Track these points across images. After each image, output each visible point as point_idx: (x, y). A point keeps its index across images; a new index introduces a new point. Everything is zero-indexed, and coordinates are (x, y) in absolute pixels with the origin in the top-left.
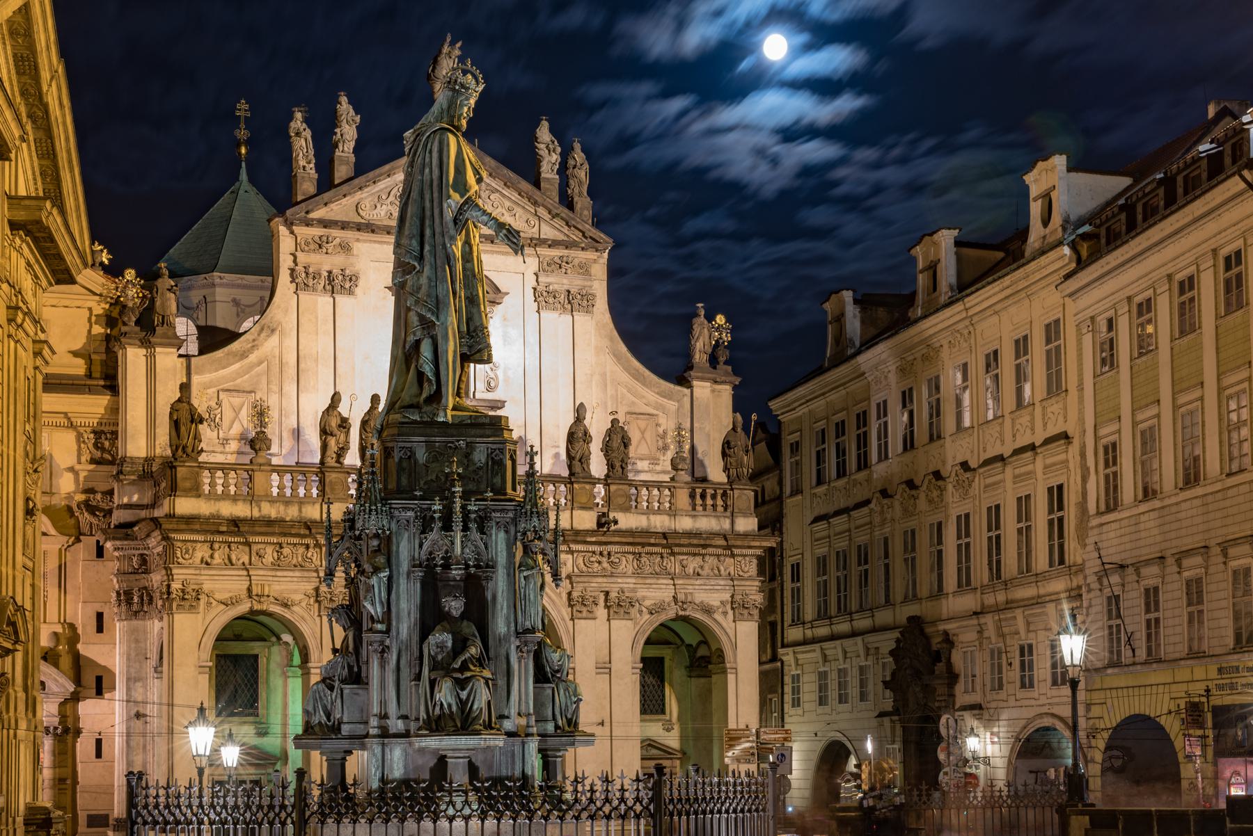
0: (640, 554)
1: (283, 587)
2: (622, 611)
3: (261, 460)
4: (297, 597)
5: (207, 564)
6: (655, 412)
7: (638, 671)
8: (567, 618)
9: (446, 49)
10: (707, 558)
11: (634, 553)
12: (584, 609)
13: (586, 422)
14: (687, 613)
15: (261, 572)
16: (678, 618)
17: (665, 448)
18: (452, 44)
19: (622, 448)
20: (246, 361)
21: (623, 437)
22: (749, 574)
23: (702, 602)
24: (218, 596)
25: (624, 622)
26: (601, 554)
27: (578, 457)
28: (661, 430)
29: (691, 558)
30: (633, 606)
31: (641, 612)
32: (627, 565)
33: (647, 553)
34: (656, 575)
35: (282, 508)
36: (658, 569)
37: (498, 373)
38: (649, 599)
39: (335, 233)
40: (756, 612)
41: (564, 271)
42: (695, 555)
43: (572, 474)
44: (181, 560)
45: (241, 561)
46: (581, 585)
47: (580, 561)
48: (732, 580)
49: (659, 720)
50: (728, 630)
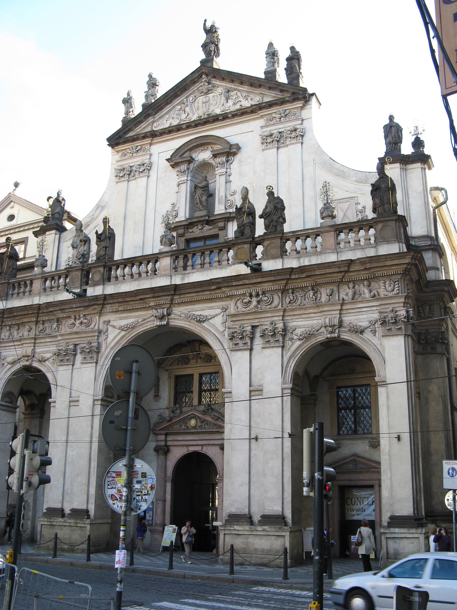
1: (41, 350)
4: (47, 355)
7: (289, 391)
10: (351, 285)
15: (28, 341)
22: (395, 291)
25: (275, 349)
26: (251, 296)
28: (360, 207)
29: (335, 288)
34: (302, 307)
35: (45, 299)
38: (299, 327)
41: (278, 120)
46: (238, 323)
47: (239, 304)
49: (366, 438)
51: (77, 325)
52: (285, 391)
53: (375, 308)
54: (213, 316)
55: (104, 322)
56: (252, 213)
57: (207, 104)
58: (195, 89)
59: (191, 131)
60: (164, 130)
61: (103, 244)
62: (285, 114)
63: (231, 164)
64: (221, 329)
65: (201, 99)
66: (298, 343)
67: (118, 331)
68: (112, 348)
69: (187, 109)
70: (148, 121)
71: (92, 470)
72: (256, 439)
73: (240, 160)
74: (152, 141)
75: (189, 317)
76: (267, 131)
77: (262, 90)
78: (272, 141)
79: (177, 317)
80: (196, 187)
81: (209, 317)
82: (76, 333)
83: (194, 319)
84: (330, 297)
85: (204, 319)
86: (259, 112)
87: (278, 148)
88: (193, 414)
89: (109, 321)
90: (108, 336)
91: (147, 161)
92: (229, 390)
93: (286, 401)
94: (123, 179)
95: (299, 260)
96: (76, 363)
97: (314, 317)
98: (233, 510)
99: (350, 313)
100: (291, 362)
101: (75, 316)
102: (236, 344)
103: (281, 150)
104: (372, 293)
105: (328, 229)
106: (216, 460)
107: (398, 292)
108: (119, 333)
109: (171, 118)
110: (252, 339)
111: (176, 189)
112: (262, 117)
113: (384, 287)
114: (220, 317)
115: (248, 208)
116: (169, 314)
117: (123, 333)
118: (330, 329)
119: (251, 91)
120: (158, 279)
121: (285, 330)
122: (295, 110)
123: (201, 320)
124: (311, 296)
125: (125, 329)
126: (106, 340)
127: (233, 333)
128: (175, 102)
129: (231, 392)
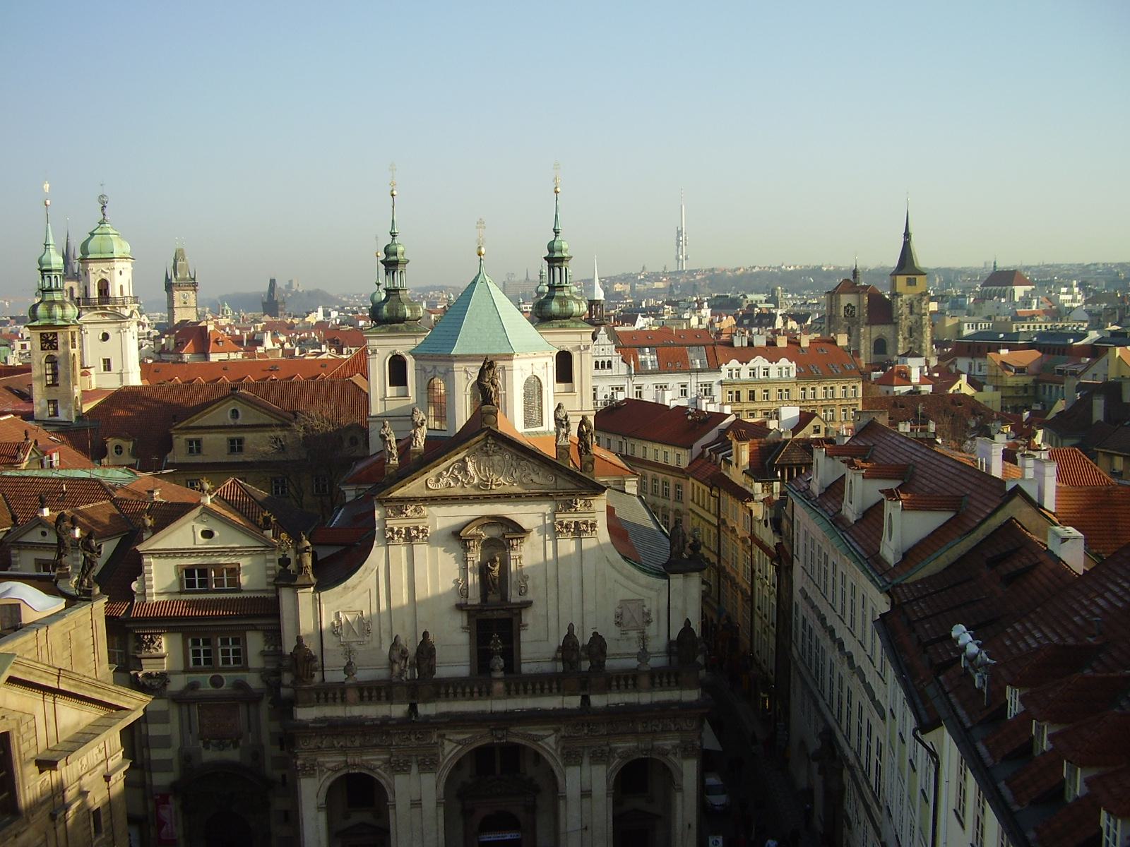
3: (350, 681)
4: (379, 763)
5: (319, 747)
6: (642, 598)
7: (612, 795)
17: (648, 622)
20: (356, 592)
24: (327, 765)
26: (583, 725)
28: (646, 610)
31: (614, 757)
32: (603, 731)
37: (527, 582)
38: (620, 748)
44: (303, 747)
45: (340, 745)
51: (413, 740)
64: (554, 747)
66: (618, 760)
67: (455, 745)
72: (586, 828)
89: (444, 735)
90: (444, 748)
92: (564, 794)
104: (677, 727)
117: (460, 747)
118: (645, 753)
120: (494, 702)
121: (610, 749)
123: (536, 739)
127: (568, 752)
129: (566, 796)
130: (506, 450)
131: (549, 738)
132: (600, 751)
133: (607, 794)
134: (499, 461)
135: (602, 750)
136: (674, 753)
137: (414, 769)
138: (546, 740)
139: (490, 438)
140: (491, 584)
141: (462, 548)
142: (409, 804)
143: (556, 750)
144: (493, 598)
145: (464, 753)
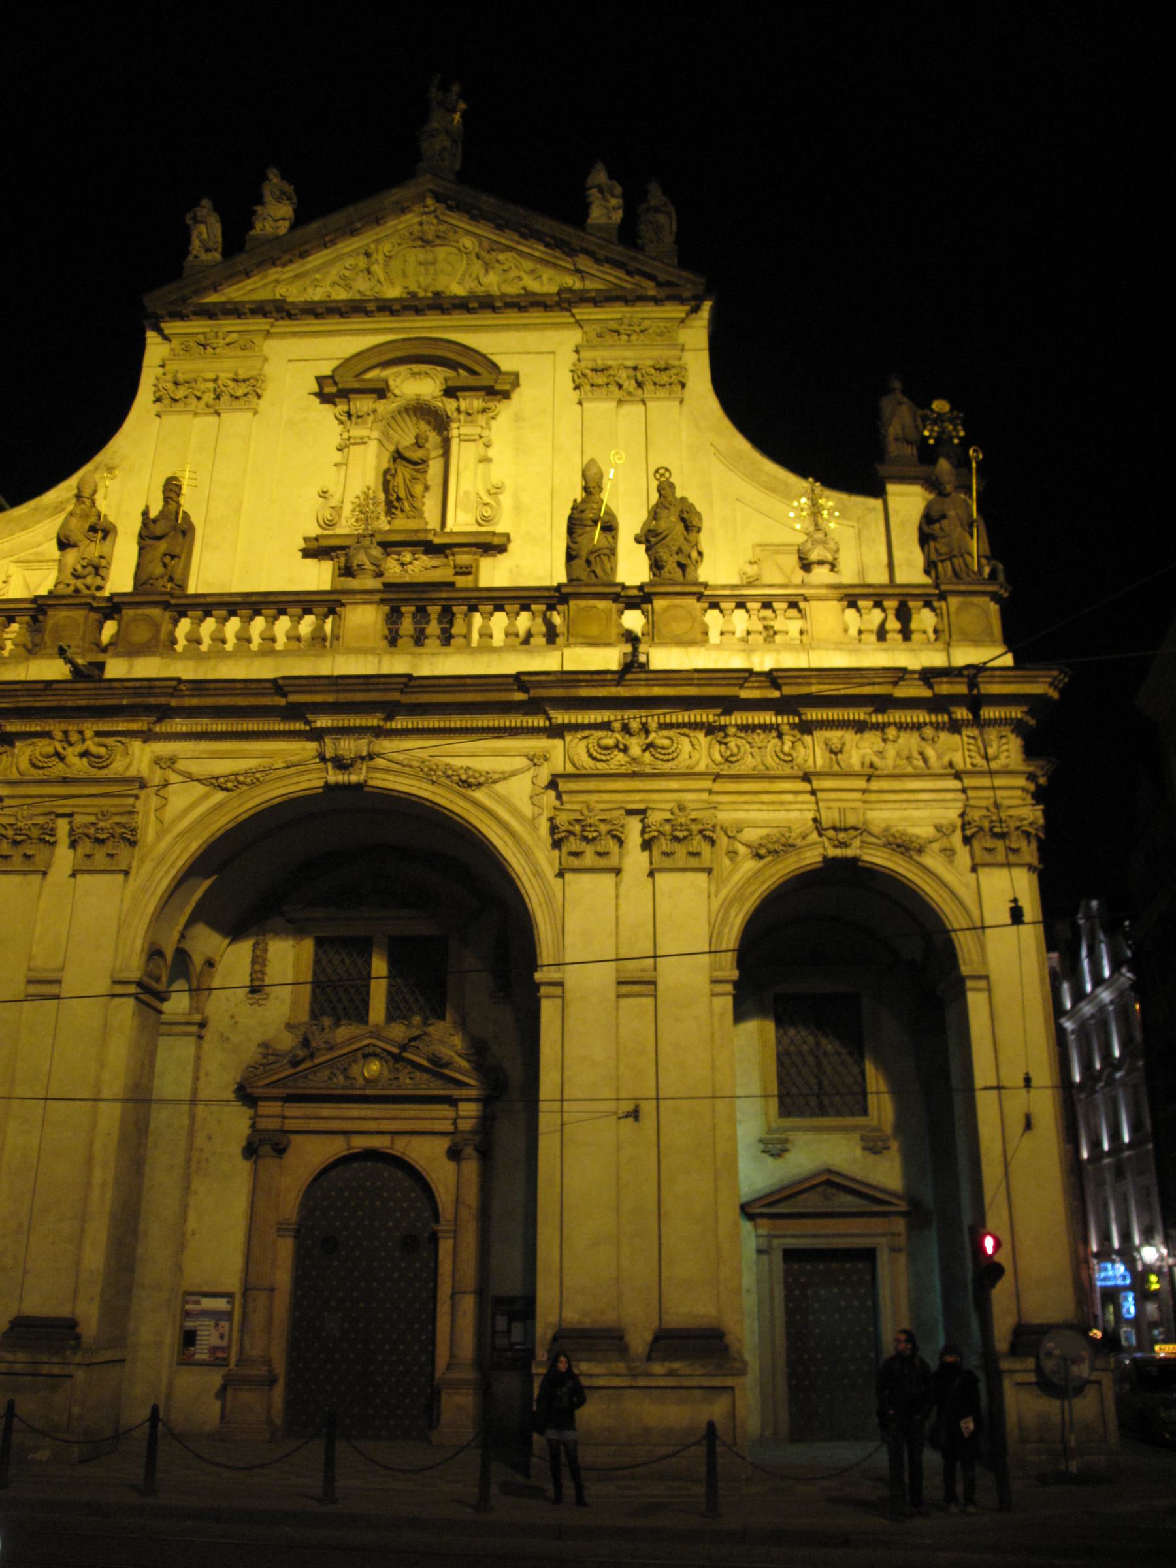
0: (723, 728)
2: (681, 850)
7: (729, 988)
8: (549, 871)
9: (434, 93)
10: (891, 732)
11: (710, 729)
12: (589, 850)
13: (605, 496)
14: (849, 852)
16: (830, 863)
18: (445, 87)
19: (680, 527)
21: (682, 511)
23: (887, 829)
25: (690, 876)
26: (626, 729)
27: (584, 554)
29: (849, 736)
30: (712, 842)
31: (732, 854)
33: (745, 728)
36: (771, 761)
38: (754, 825)
39: (229, 325)
40: (1030, 853)
41: (624, 337)
42: (860, 727)
43: (570, 580)
46: (582, 797)
48: (958, 776)
49: (854, 1128)
50: (961, 891)
52: (720, 988)
53: (950, 796)
54: (507, 775)
55: (157, 761)
56: (610, 528)
57: (431, 269)
58: (400, 227)
59: (385, 321)
60: (312, 306)
61: (163, 546)
62: (642, 327)
63: (493, 418)
64: (527, 810)
65: (417, 255)
67: (200, 789)
68: (181, 834)
69: (377, 269)
70: (265, 276)
71: (96, 1194)
73: (516, 414)
74: (272, 325)
75: (429, 774)
76: (602, 356)
77: (584, 262)
78: (607, 384)
79: (397, 767)
80: (398, 456)
81: (496, 776)
82: (65, 781)
83: (448, 777)
84: (840, 756)
85: (482, 780)
86: (574, 311)
87: (620, 402)
88: (374, 1045)
91: (254, 373)
93: (722, 1015)
94: (179, 406)
95: (749, 656)
96: (52, 871)
97: (791, 803)
98: (572, 1316)
99: (885, 801)
100: (733, 913)
101: (66, 733)
102: (576, 854)
103: (627, 409)
104: (946, 760)
105: (823, 591)
106: (434, 1176)
107: (1008, 761)
108: (205, 797)
109: (328, 283)
110: (621, 842)
111: (338, 457)
112: (579, 324)
113: (972, 747)
114: (528, 776)
115: (605, 513)
116: (371, 757)
119: (553, 260)
122: (668, 325)
123: (467, 783)
124: (786, 748)
125: (230, 785)
126: (158, 814)
128: (347, 246)
130: (468, 232)
131: (513, 780)
132: (683, 820)
133: (714, 981)
134: (450, 254)
135: (694, 820)
136: (944, 850)
137: (64, 857)
138: (499, 787)
139: (430, 201)
140: (402, 494)
141: (341, 423)
142: (22, 979)
143: (532, 823)
144: (401, 523)
145: (220, 823)
